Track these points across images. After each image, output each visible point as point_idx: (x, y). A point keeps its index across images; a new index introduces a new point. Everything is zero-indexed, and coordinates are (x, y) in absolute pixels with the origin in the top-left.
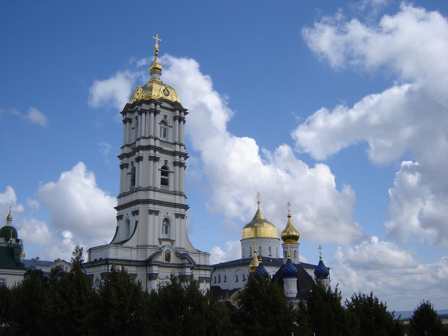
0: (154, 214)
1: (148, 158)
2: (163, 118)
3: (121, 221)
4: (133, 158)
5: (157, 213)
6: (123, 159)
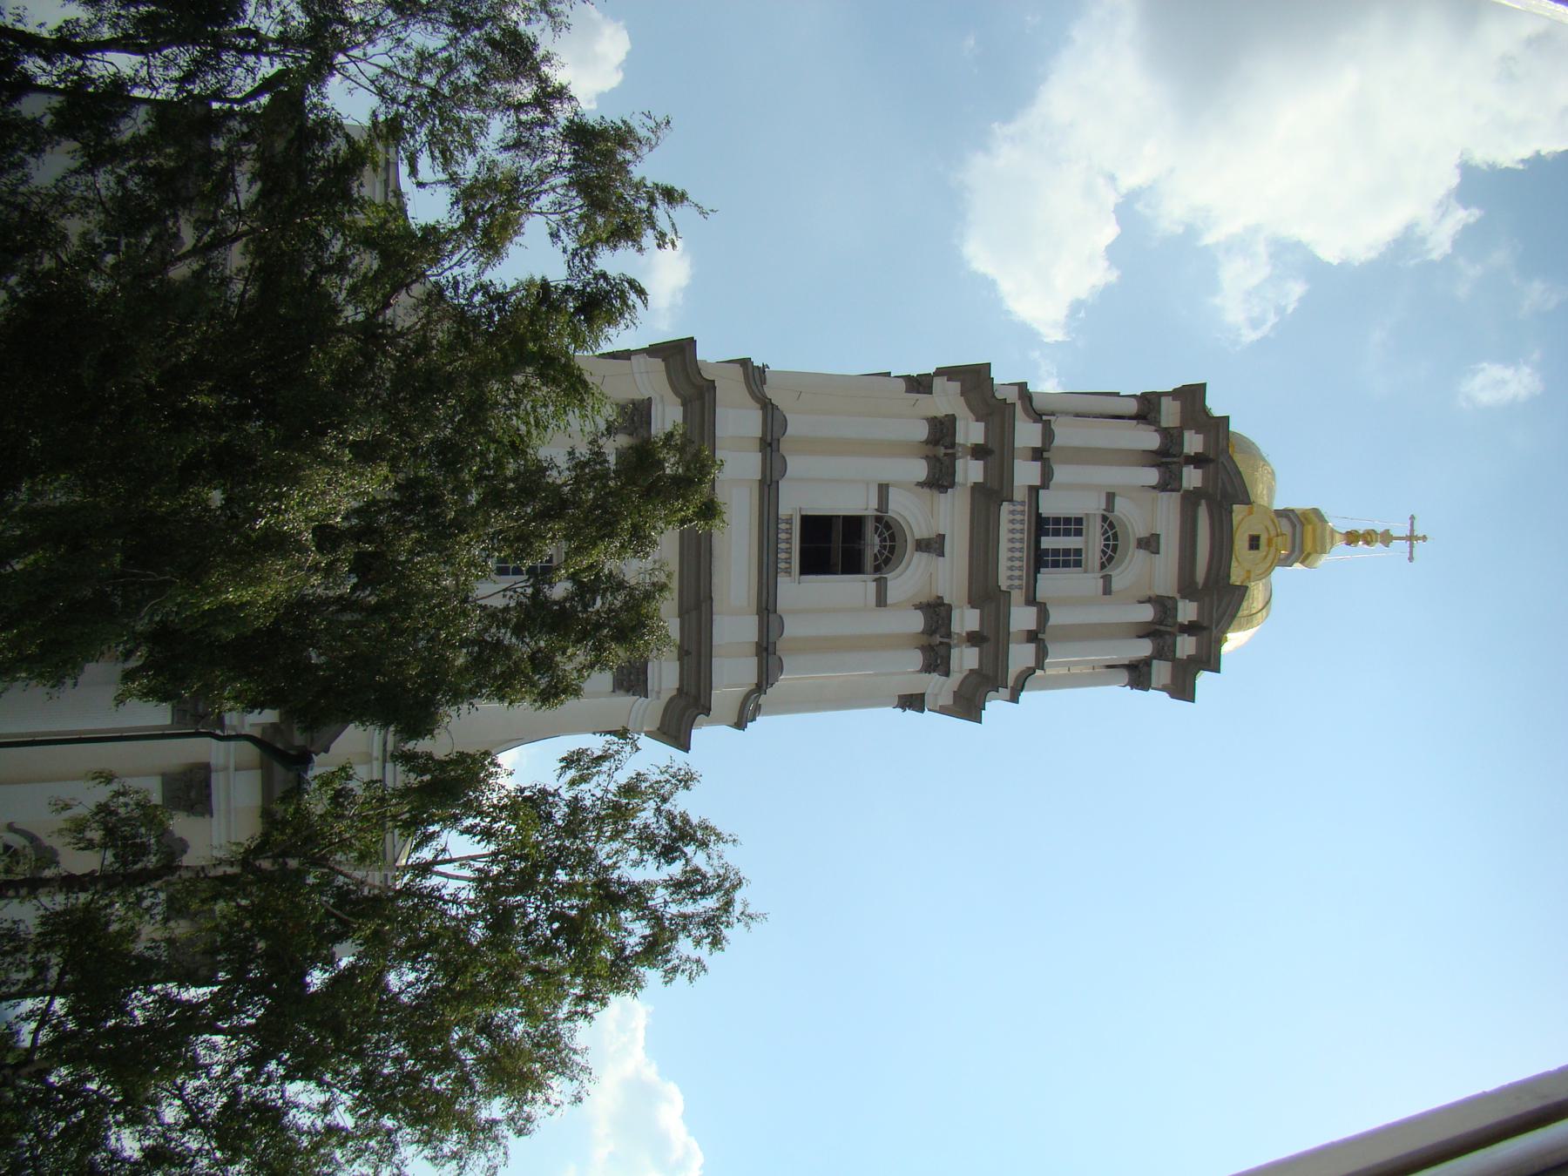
2: (1142, 532)
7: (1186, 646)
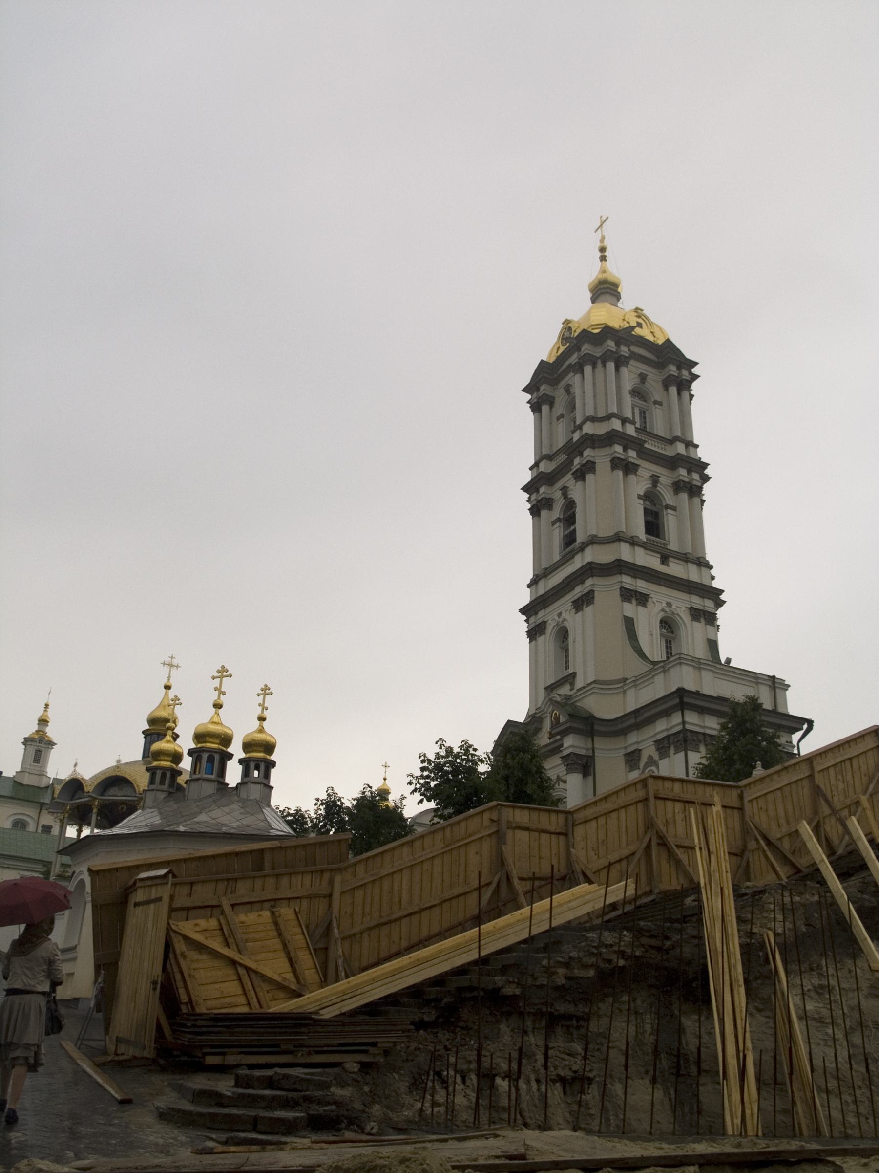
0: (634, 601)
1: (609, 464)
2: (637, 381)
3: (541, 639)
4: (568, 480)
5: (642, 599)
6: (537, 491)
7: (685, 373)
